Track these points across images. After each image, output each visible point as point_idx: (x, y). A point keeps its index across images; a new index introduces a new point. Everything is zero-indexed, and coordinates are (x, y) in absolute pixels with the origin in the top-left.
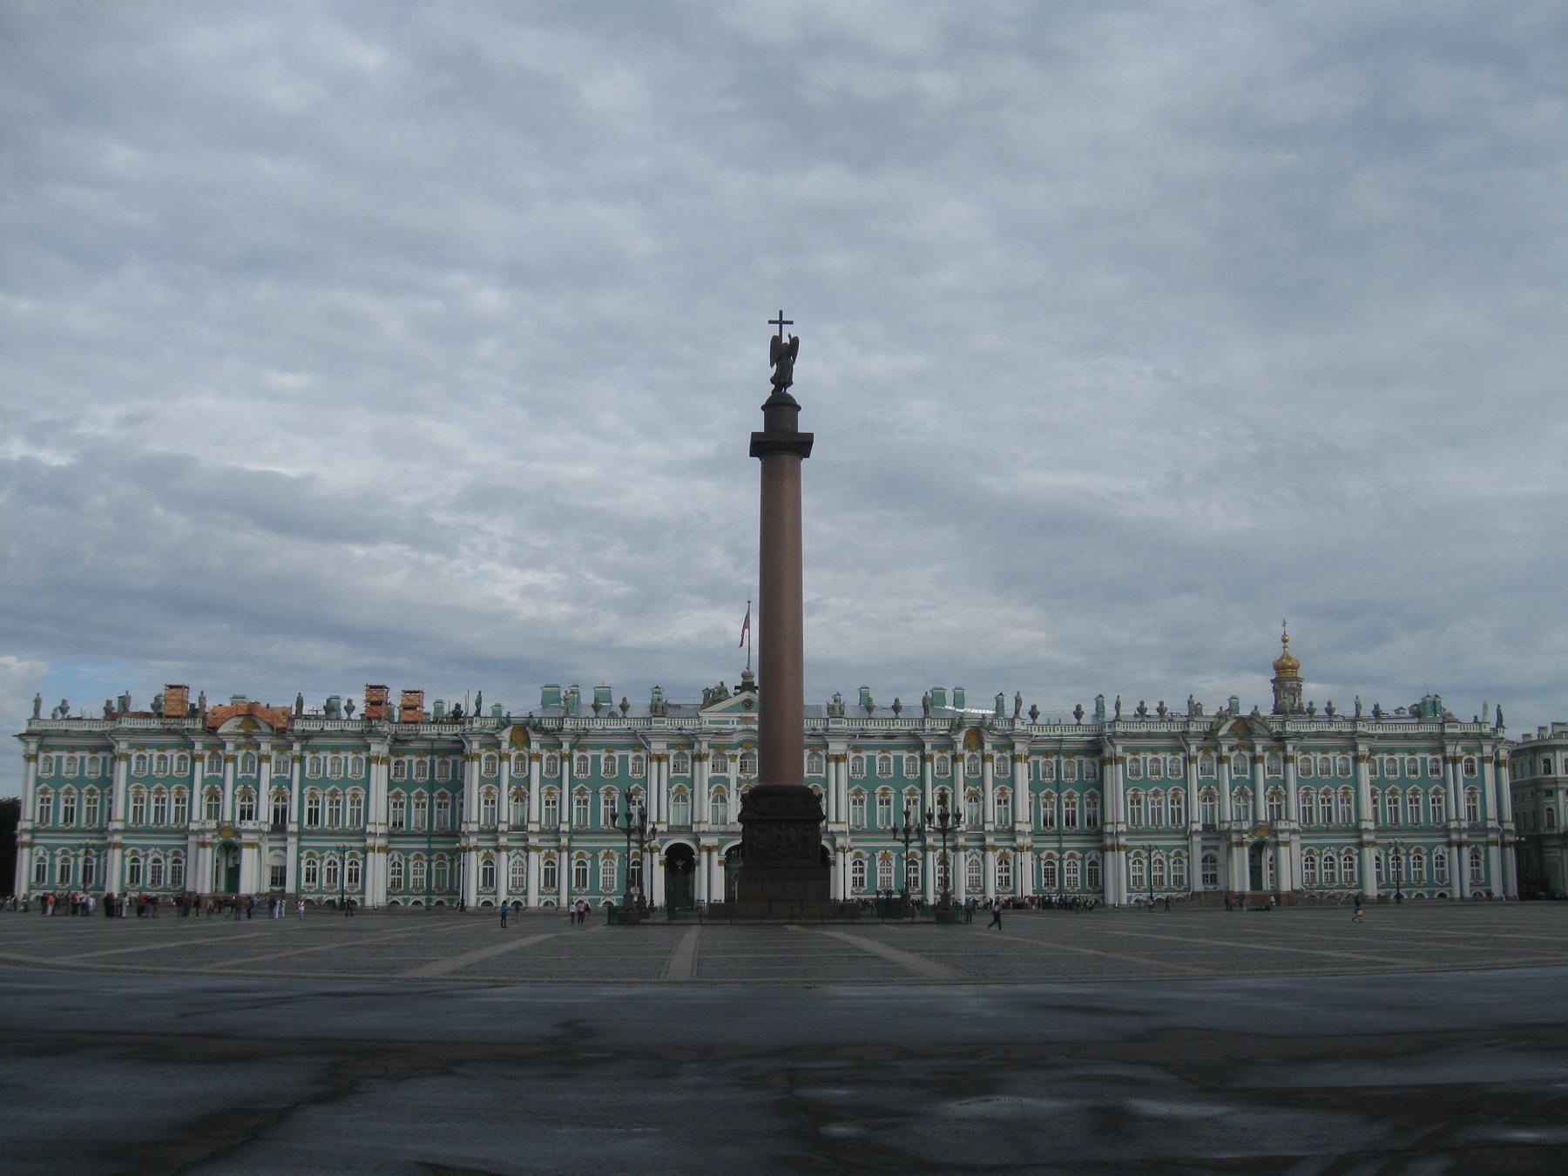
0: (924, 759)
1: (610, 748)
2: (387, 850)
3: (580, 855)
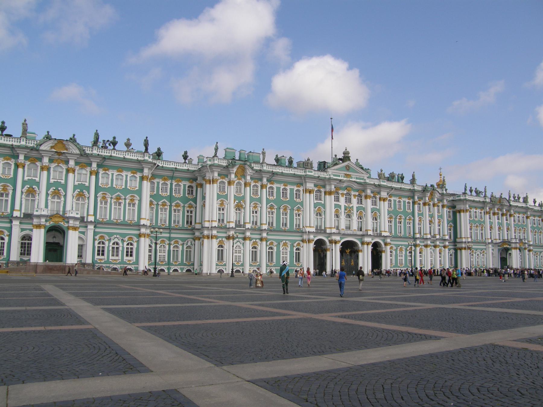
0: (414, 203)
1: (286, 184)
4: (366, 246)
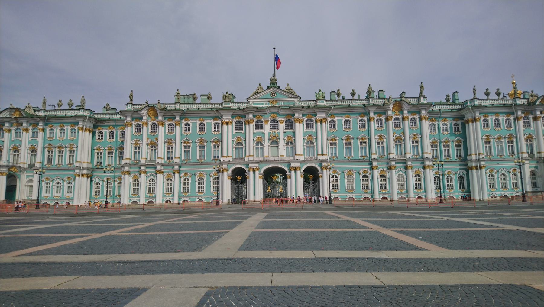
0: (369, 120)
2: (90, 176)
3: (186, 175)
4: (293, 172)
